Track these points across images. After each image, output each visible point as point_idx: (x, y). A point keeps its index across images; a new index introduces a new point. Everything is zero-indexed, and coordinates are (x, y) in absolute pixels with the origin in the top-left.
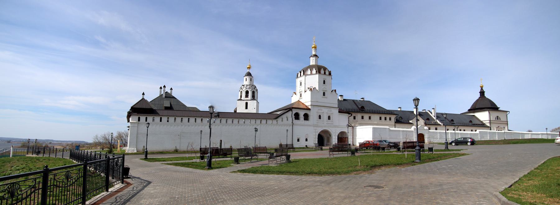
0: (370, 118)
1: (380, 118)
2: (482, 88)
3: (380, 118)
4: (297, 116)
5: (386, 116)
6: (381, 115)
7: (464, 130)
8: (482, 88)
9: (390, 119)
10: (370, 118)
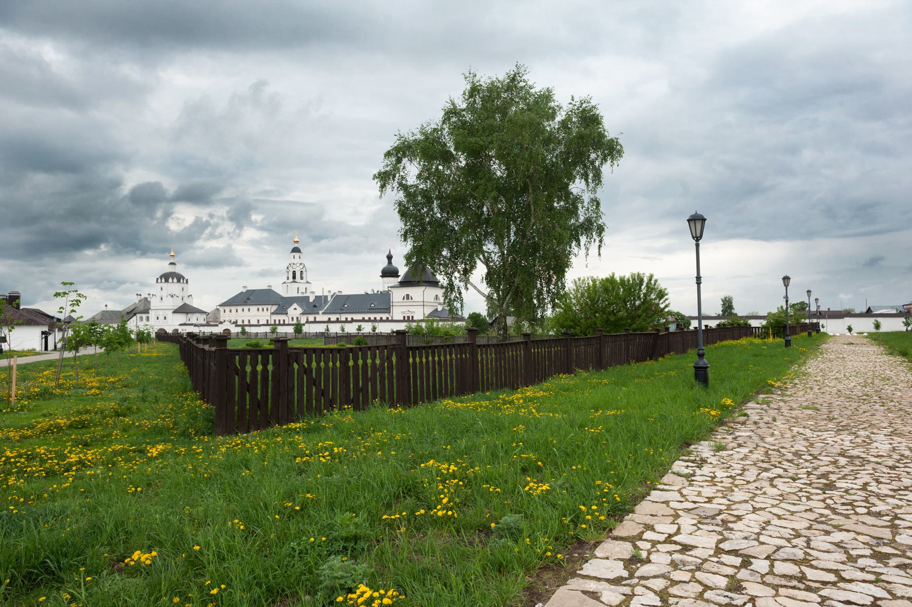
4: (141, 319)
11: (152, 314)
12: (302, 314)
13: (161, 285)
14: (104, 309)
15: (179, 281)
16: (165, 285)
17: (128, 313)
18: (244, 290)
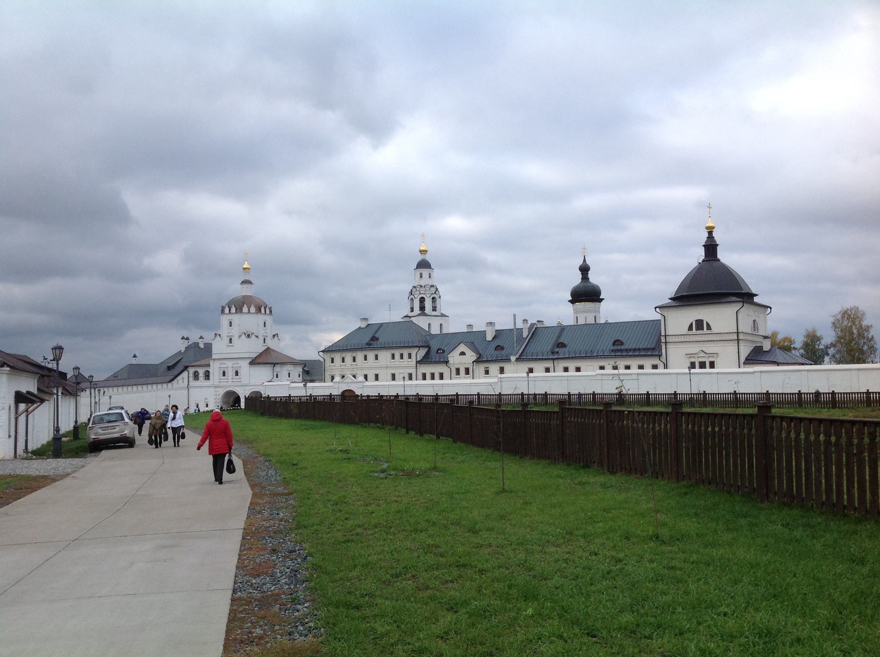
0: (376, 357)
1: (393, 357)
2: (710, 233)
3: (393, 357)
4: (196, 376)
5: (402, 351)
6: (393, 351)
7: (578, 369)
8: (710, 233)
9: (410, 356)
10: (376, 357)
11: (215, 369)
12: (477, 361)
13: (230, 317)
14: (134, 361)
16: (236, 318)
17: (169, 368)
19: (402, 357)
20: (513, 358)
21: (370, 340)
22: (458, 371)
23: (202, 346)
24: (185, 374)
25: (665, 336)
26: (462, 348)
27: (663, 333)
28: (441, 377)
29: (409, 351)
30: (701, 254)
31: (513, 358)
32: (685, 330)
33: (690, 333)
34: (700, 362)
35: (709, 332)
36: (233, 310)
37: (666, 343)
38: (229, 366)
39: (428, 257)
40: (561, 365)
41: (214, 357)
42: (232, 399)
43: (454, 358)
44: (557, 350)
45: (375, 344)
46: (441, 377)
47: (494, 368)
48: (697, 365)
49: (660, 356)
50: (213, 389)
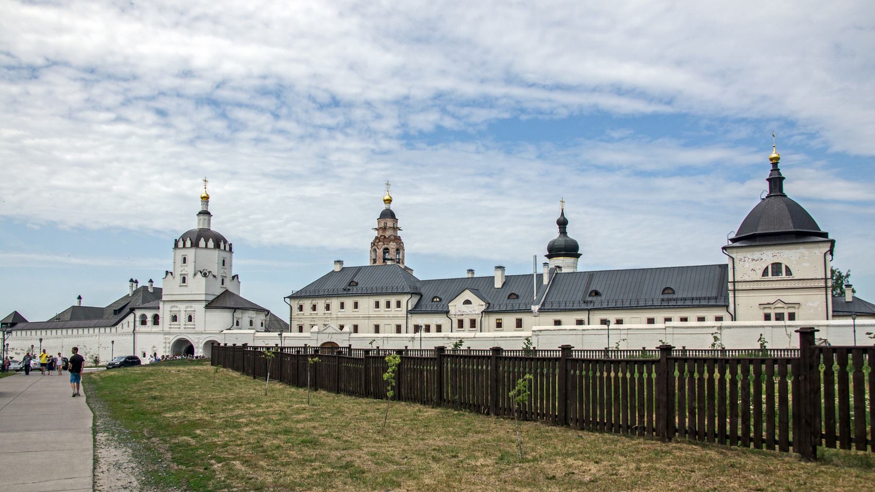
0: (356, 305)
1: (377, 305)
2: (775, 165)
3: (377, 305)
5: (388, 298)
6: (377, 298)
7: (619, 322)
8: (775, 165)
9: (399, 304)
10: (356, 305)
11: (165, 312)
15: (217, 246)
16: (191, 253)
18: (337, 268)
19: (388, 305)
20: (535, 308)
21: (344, 284)
22: (461, 324)
23: (151, 290)
24: (131, 316)
25: (734, 282)
26: (467, 295)
27: (731, 279)
28: (439, 329)
29: (399, 298)
30: (764, 188)
31: (535, 308)
32: (758, 276)
33: (766, 278)
34: (776, 314)
35: (787, 278)
36: (188, 243)
37: (734, 290)
38: (182, 310)
39: (393, 207)
40: (597, 316)
41: (164, 298)
42: (184, 348)
43: (456, 306)
44: (590, 299)
45: (354, 290)
46: (439, 329)
47: (509, 320)
48: (773, 317)
49: (727, 306)
50: (162, 336)
